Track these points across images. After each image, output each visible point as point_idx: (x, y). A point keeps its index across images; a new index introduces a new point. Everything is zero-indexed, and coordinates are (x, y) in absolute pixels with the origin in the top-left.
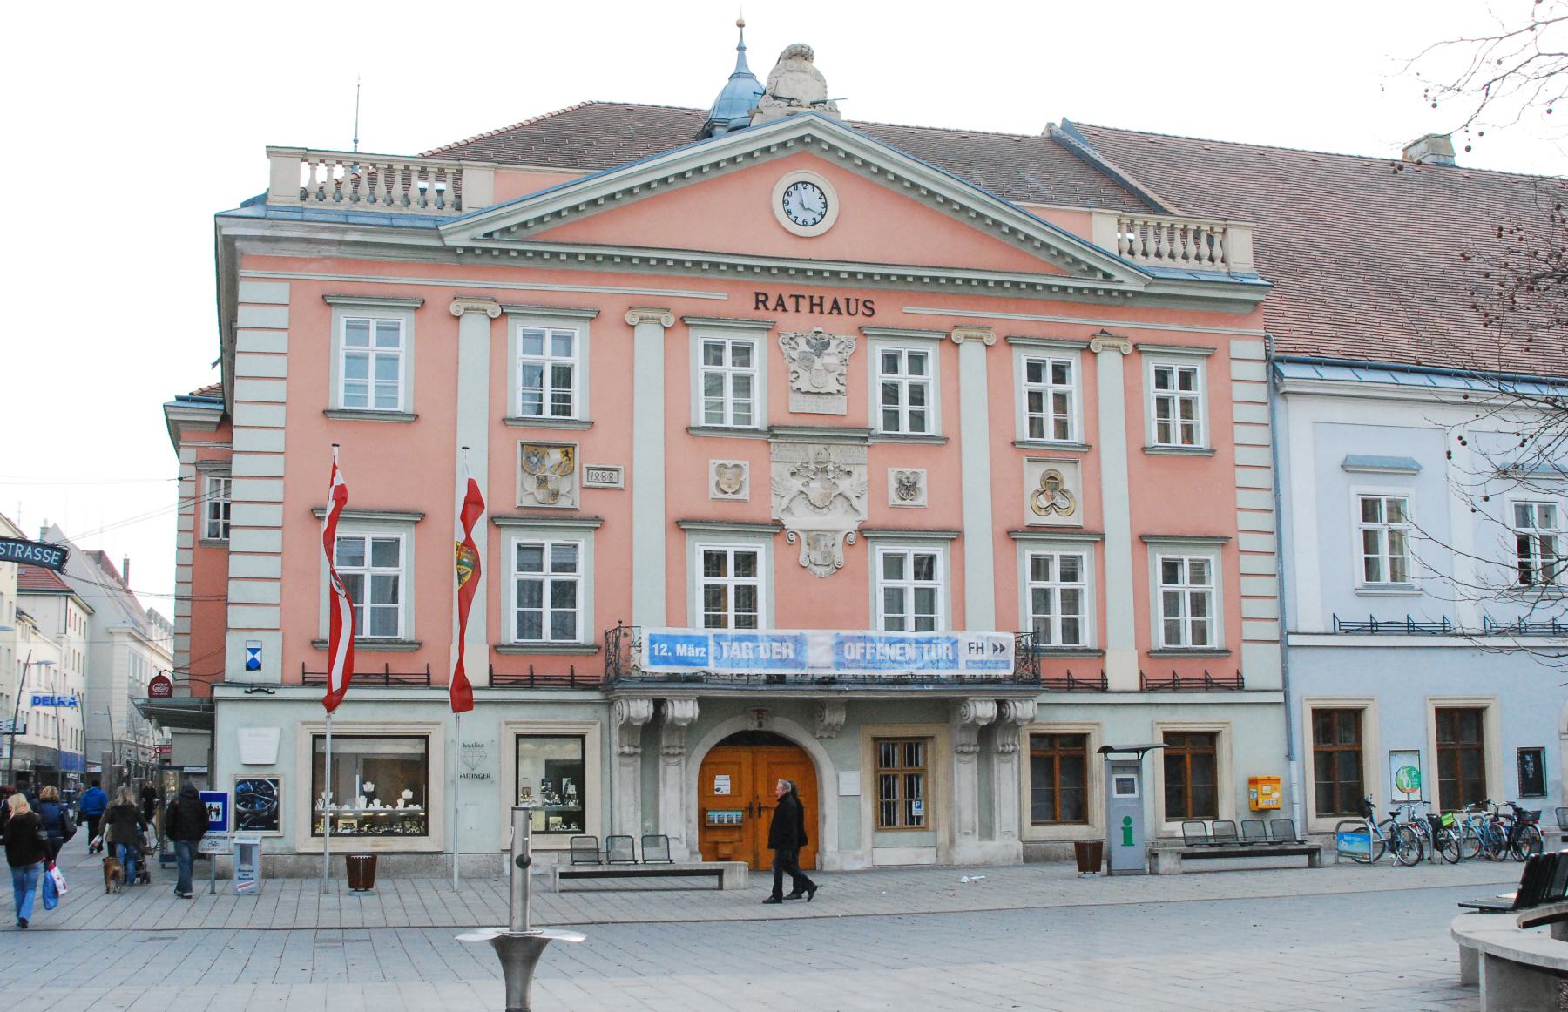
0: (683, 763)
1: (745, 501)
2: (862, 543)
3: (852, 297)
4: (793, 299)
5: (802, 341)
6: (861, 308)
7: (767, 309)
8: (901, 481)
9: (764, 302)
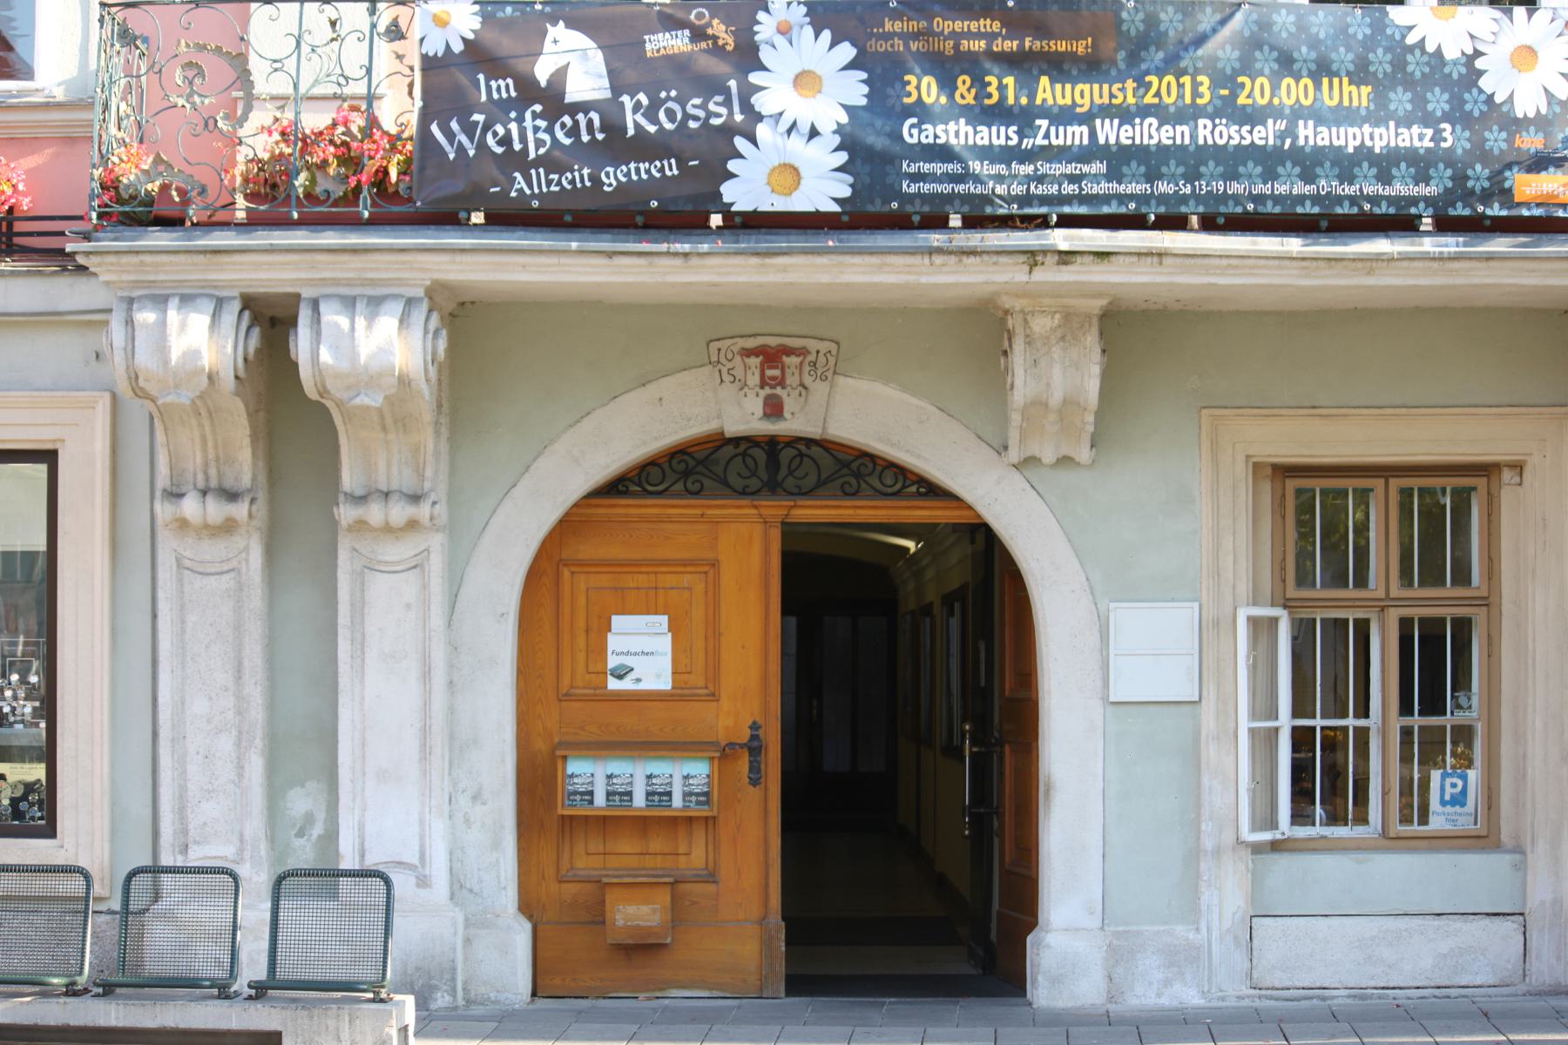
0: (436, 563)
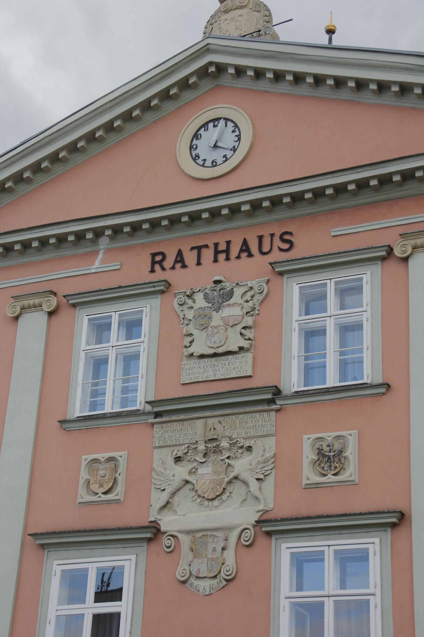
1: (117, 501)
2: (262, 541)
3: (266, 233)
4: (195, 252)
5: (199, 298)
6: (277, 242)
7: (163, 269)
8: (320, 452)
9: (160, 263)
